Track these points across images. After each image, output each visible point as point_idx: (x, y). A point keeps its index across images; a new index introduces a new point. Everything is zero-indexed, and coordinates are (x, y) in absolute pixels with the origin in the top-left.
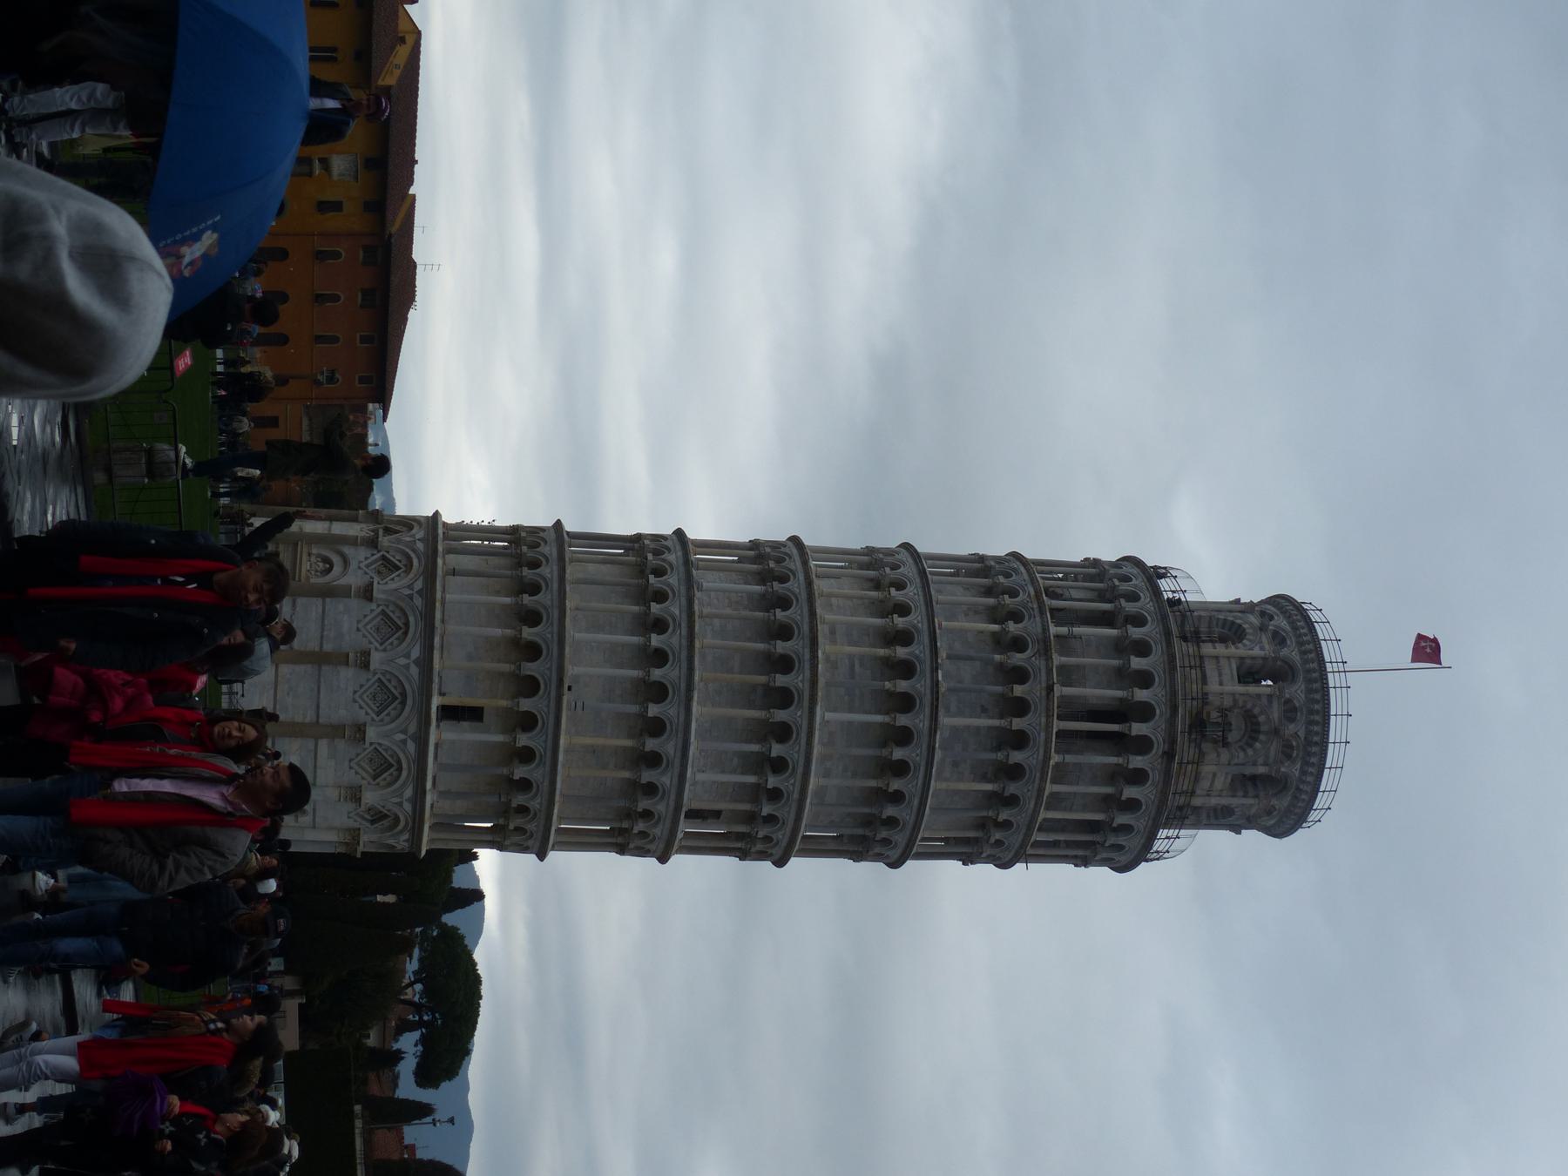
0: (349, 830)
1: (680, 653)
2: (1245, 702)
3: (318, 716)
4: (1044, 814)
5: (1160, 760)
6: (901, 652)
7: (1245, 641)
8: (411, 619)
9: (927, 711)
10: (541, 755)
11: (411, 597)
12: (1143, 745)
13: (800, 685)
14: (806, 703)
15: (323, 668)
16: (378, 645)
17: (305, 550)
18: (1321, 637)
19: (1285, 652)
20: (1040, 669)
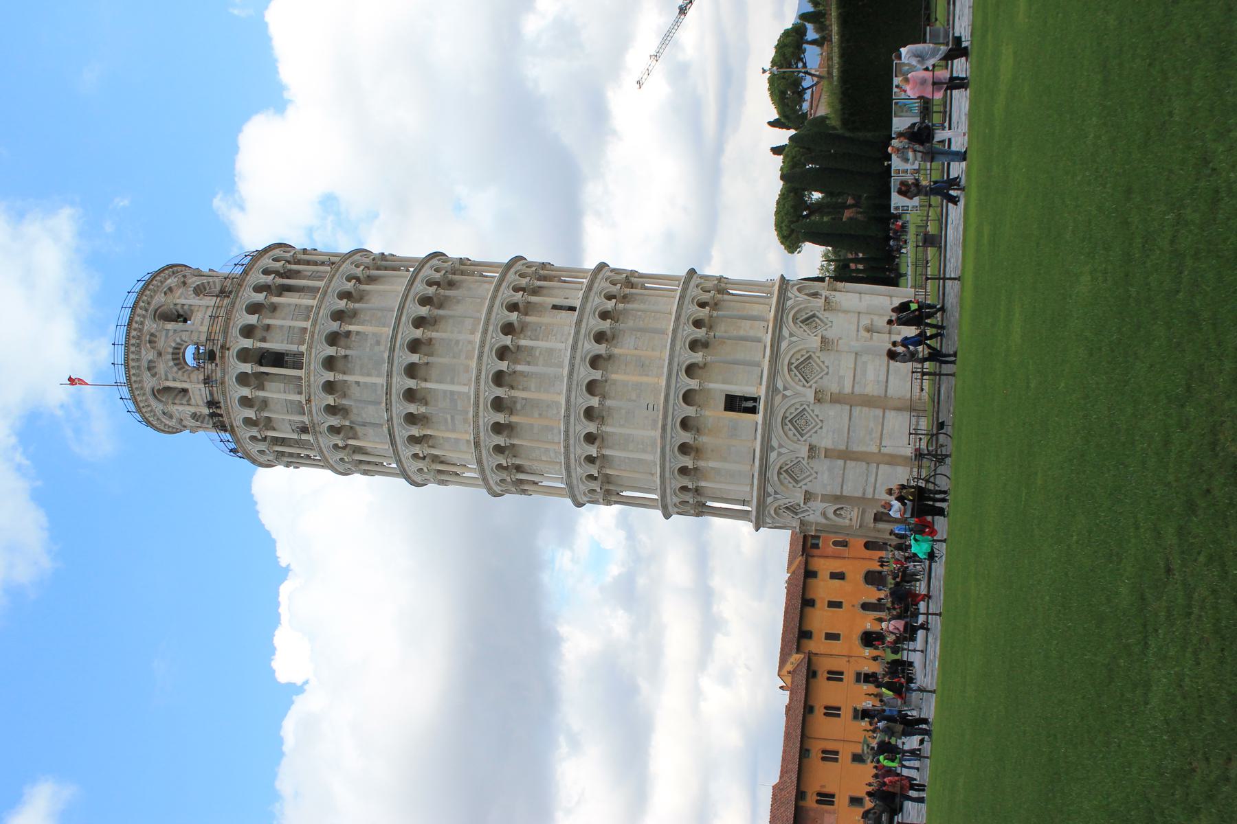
3: (851, 410)
4: (314, 303)
6: (415, 431)
8: (776, 478)
9: (394, 390)
10: (681, 371)
12: (244, 355)
14: (481, 400)
15: (844, 448)
16: (802, 460)
17: (854, 522)
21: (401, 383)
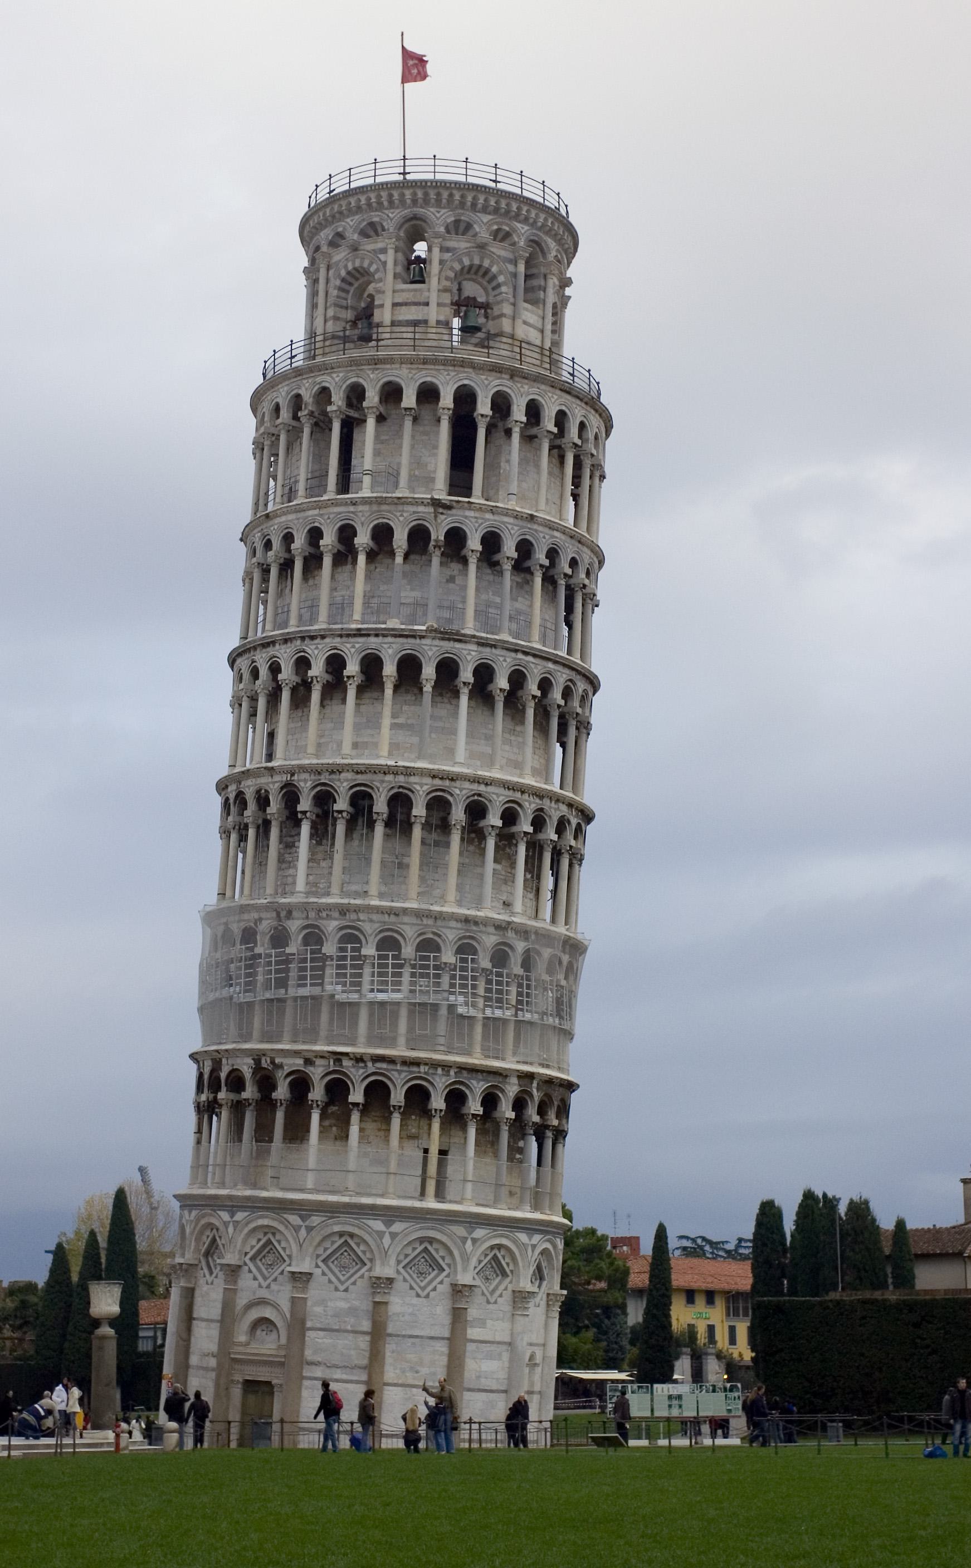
0: (548, 1305)
1: (384, 922)
2: (447, 278)
3: (443, 1338)
5: (519, 385)
7: (372, 269)
8: (337, 1228)
9: (458, 645)
11: (310, 1229)
12: (501, 405)
13: (425, 788)
15: (390, 1330)
18: (370, 181)
19: (390, 226)
20: (414, 512)
21: (469, 658)
